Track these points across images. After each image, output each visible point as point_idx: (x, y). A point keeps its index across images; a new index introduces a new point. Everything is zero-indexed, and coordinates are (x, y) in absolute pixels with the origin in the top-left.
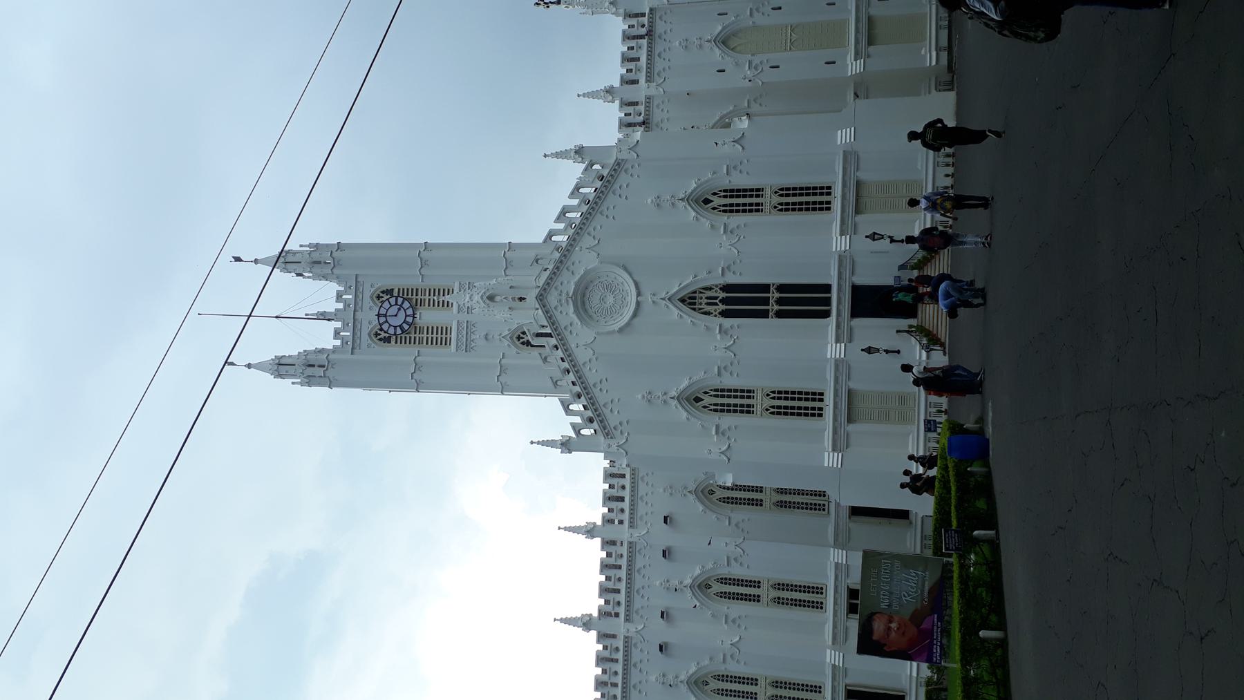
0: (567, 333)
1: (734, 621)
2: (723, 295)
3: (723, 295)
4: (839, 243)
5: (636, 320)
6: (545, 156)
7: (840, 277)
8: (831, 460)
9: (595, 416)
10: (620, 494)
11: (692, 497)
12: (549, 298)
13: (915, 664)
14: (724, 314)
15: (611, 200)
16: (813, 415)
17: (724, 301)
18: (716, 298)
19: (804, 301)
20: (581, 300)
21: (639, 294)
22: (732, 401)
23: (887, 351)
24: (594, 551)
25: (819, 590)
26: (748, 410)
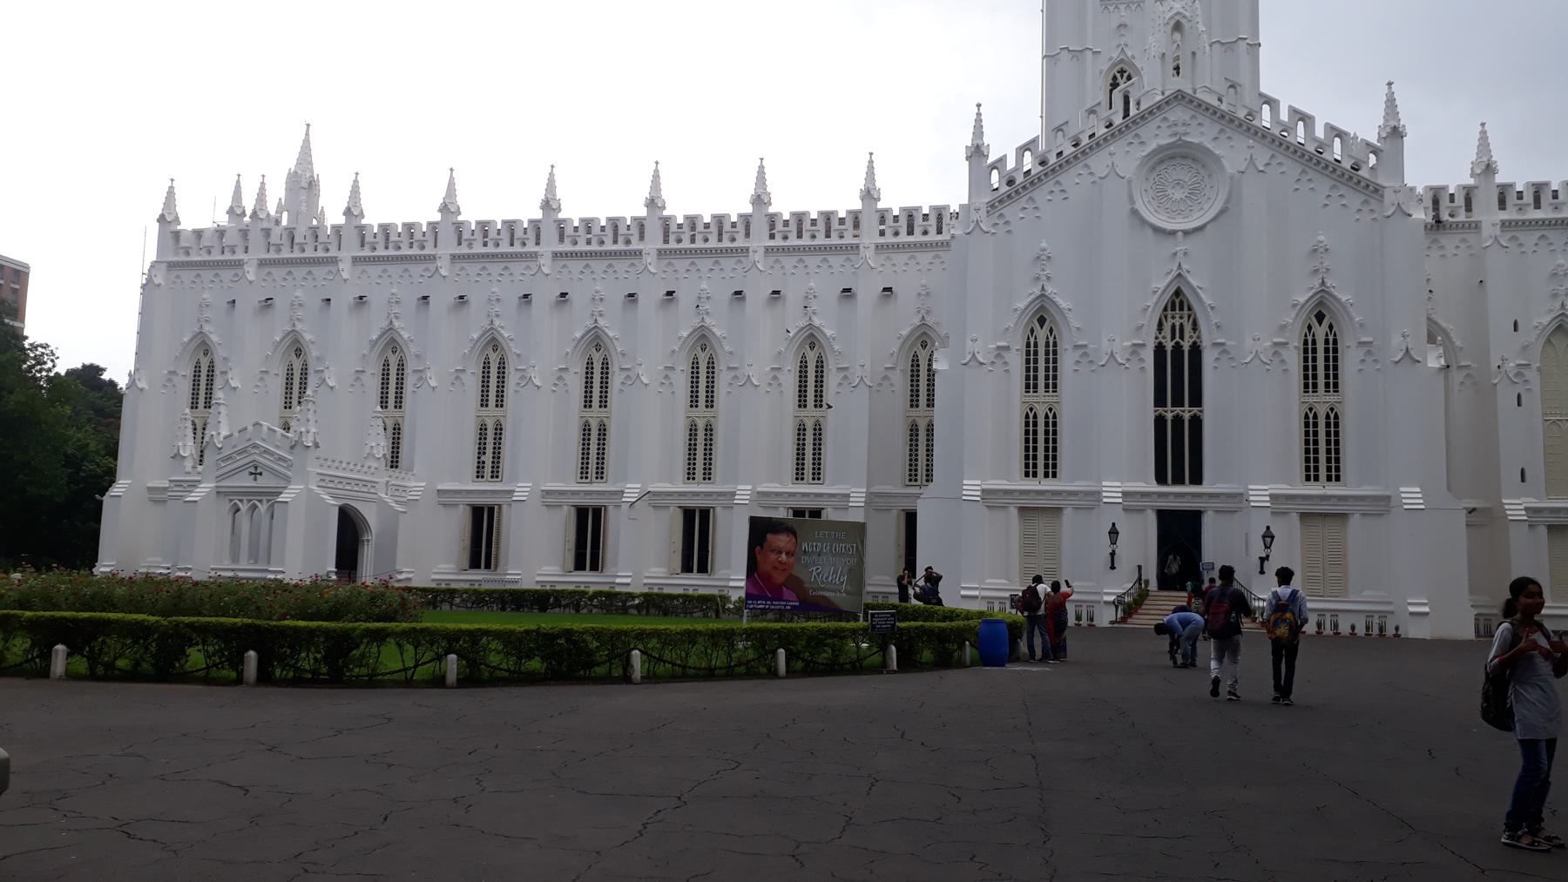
0: (1129, 138)
1: (775, 378)
2: (1186, 346)
3: (1186, 346)
4: (1259, 494)
5: (1150, 232)
6: (1390, 84)
7: (1211, 495)
8: (972, 487)
9: (1017, 188)
10: (918, 230)
11: (917, 321)
12: (1180, 108)
13: (743, 584)
14: (1159, 350)
15: (1323, 185)
16: (1027, 466)
17: (1178, 349)
18: (1182, 337)
19: (1179, 450)
20: (1178, 154)
21: (1186, 233)
22: (1041, 365)
23: (1113, 554)
24: (846, 202)
25: (817, 476)
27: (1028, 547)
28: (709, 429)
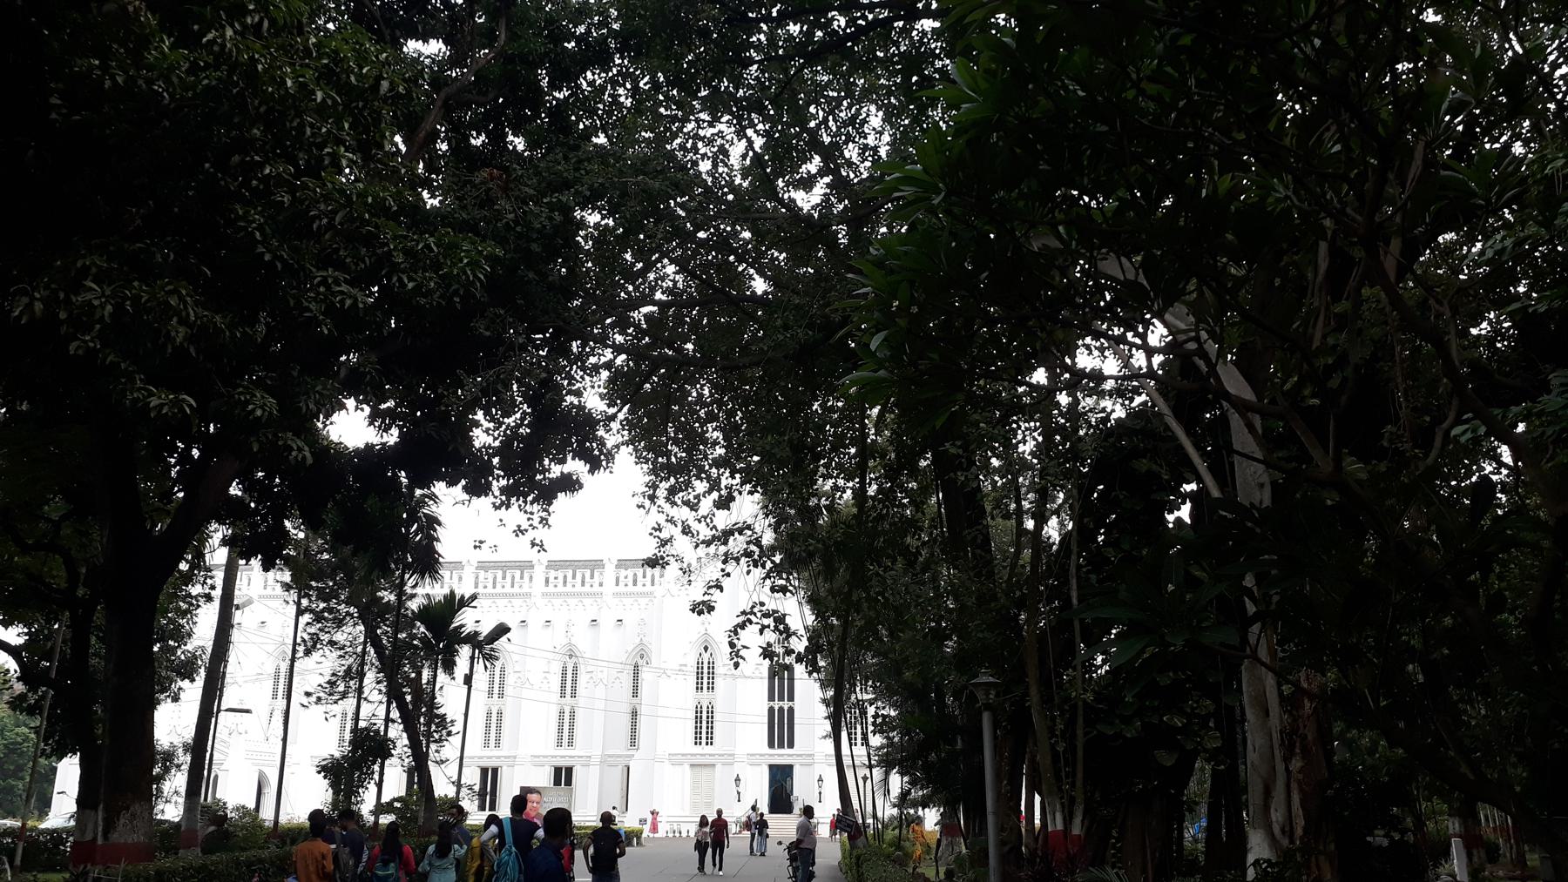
11: (638, 641)
26: (699, 688)
27: (695, 785)
28: (500, 713)
